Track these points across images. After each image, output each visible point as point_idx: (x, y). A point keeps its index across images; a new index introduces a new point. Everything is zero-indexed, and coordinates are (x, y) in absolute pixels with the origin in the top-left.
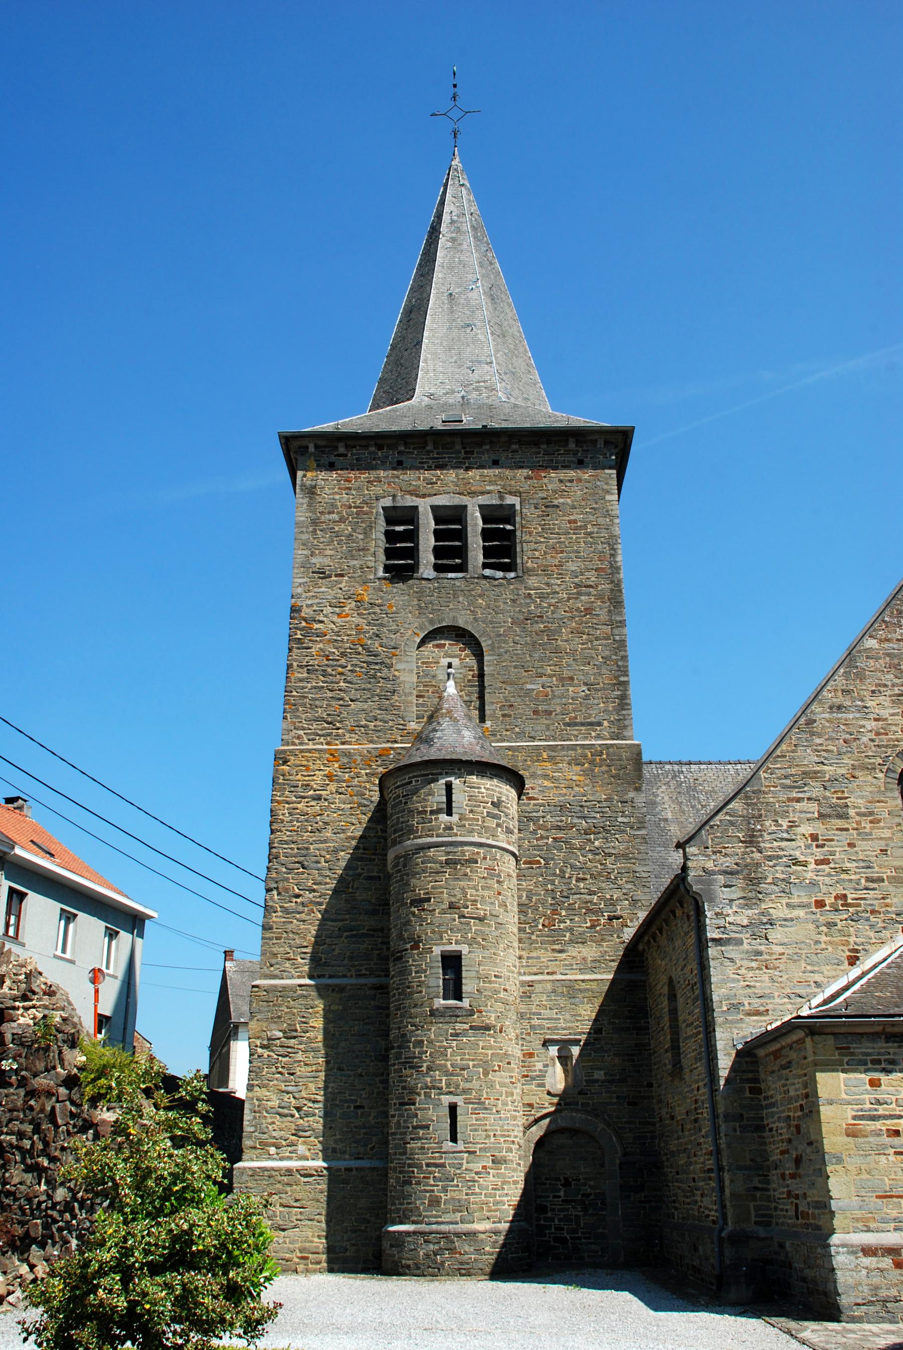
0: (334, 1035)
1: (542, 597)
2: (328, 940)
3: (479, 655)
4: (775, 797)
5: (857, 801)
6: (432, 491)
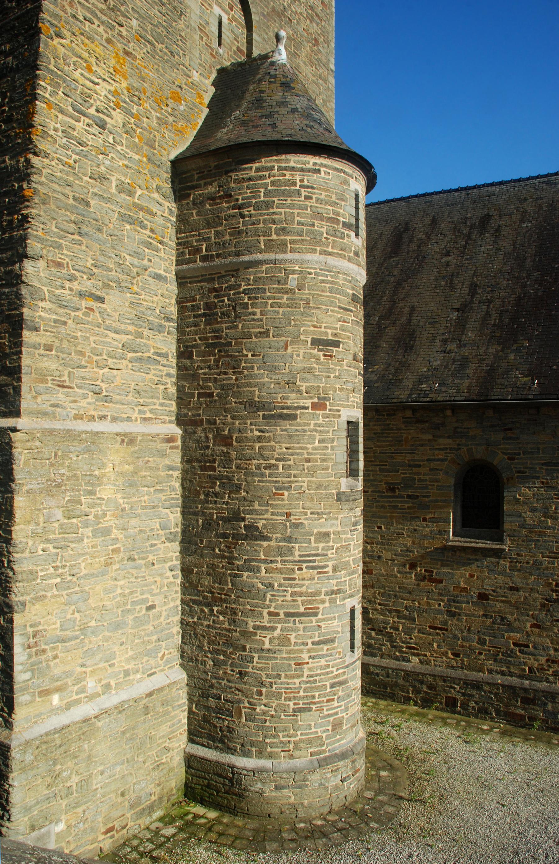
0: (123, 510)
2: (110, 360)
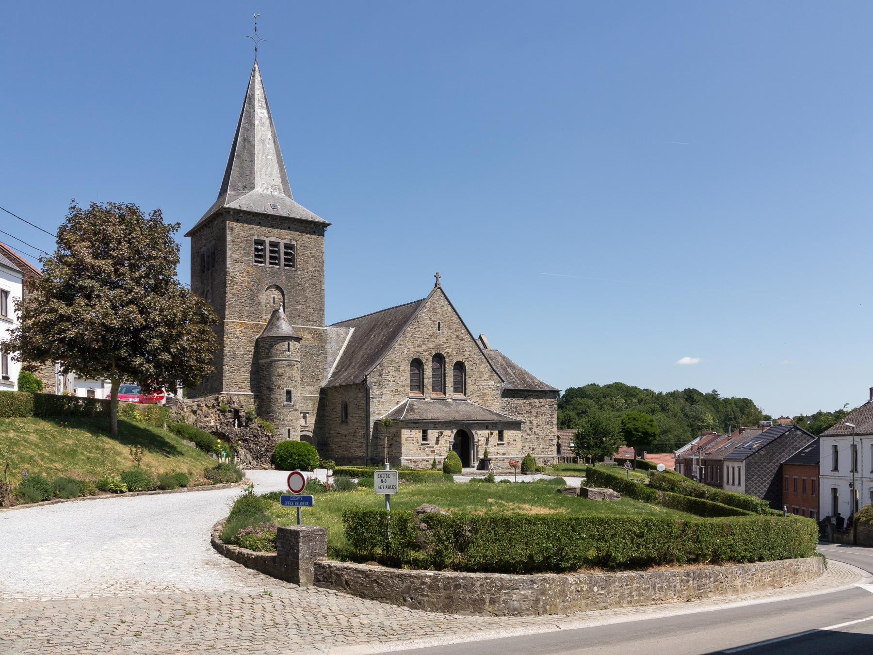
1: (302, 278)
3: (283, 295)
4: (386, 365)
5: (402, 367)
6: (272, 235)
